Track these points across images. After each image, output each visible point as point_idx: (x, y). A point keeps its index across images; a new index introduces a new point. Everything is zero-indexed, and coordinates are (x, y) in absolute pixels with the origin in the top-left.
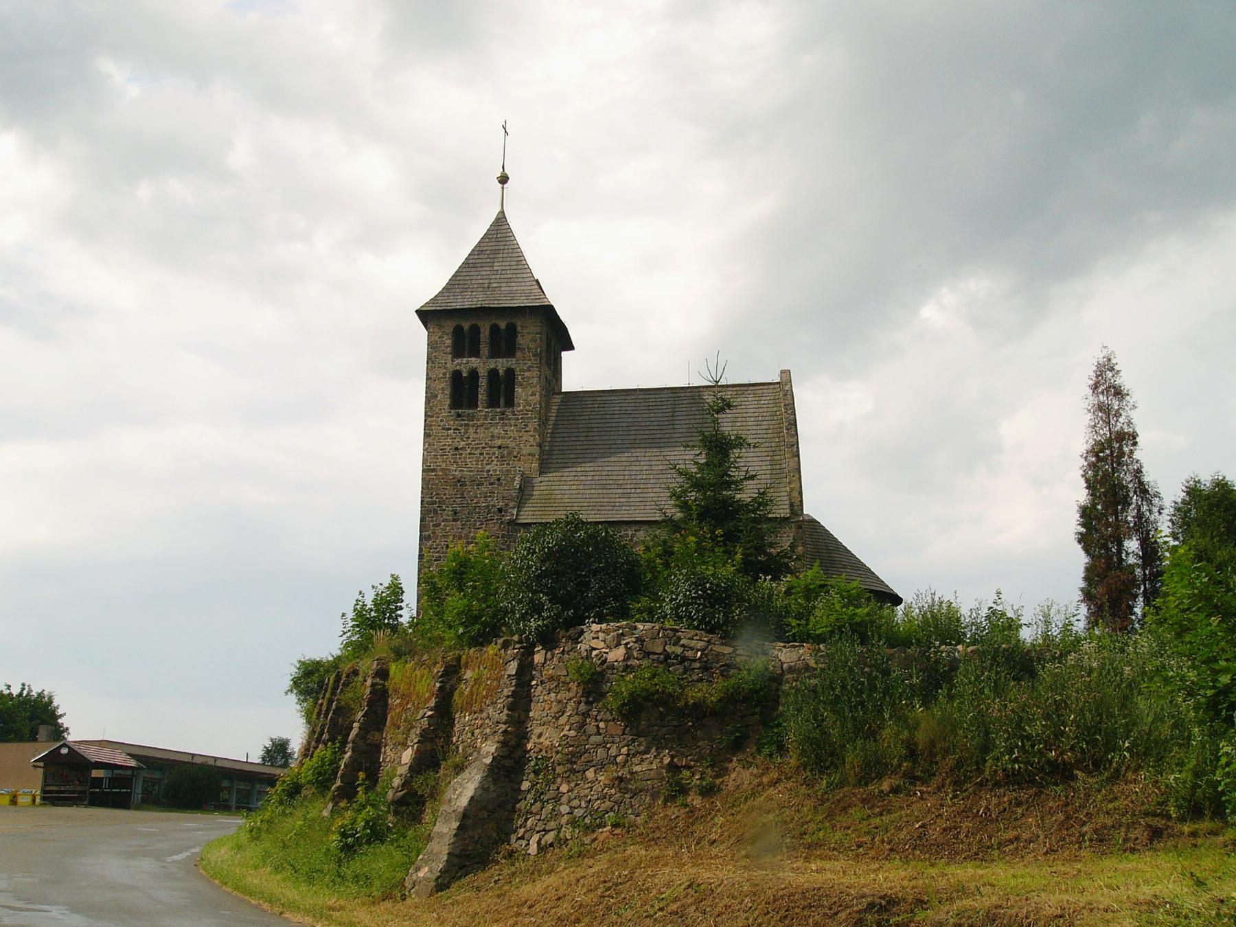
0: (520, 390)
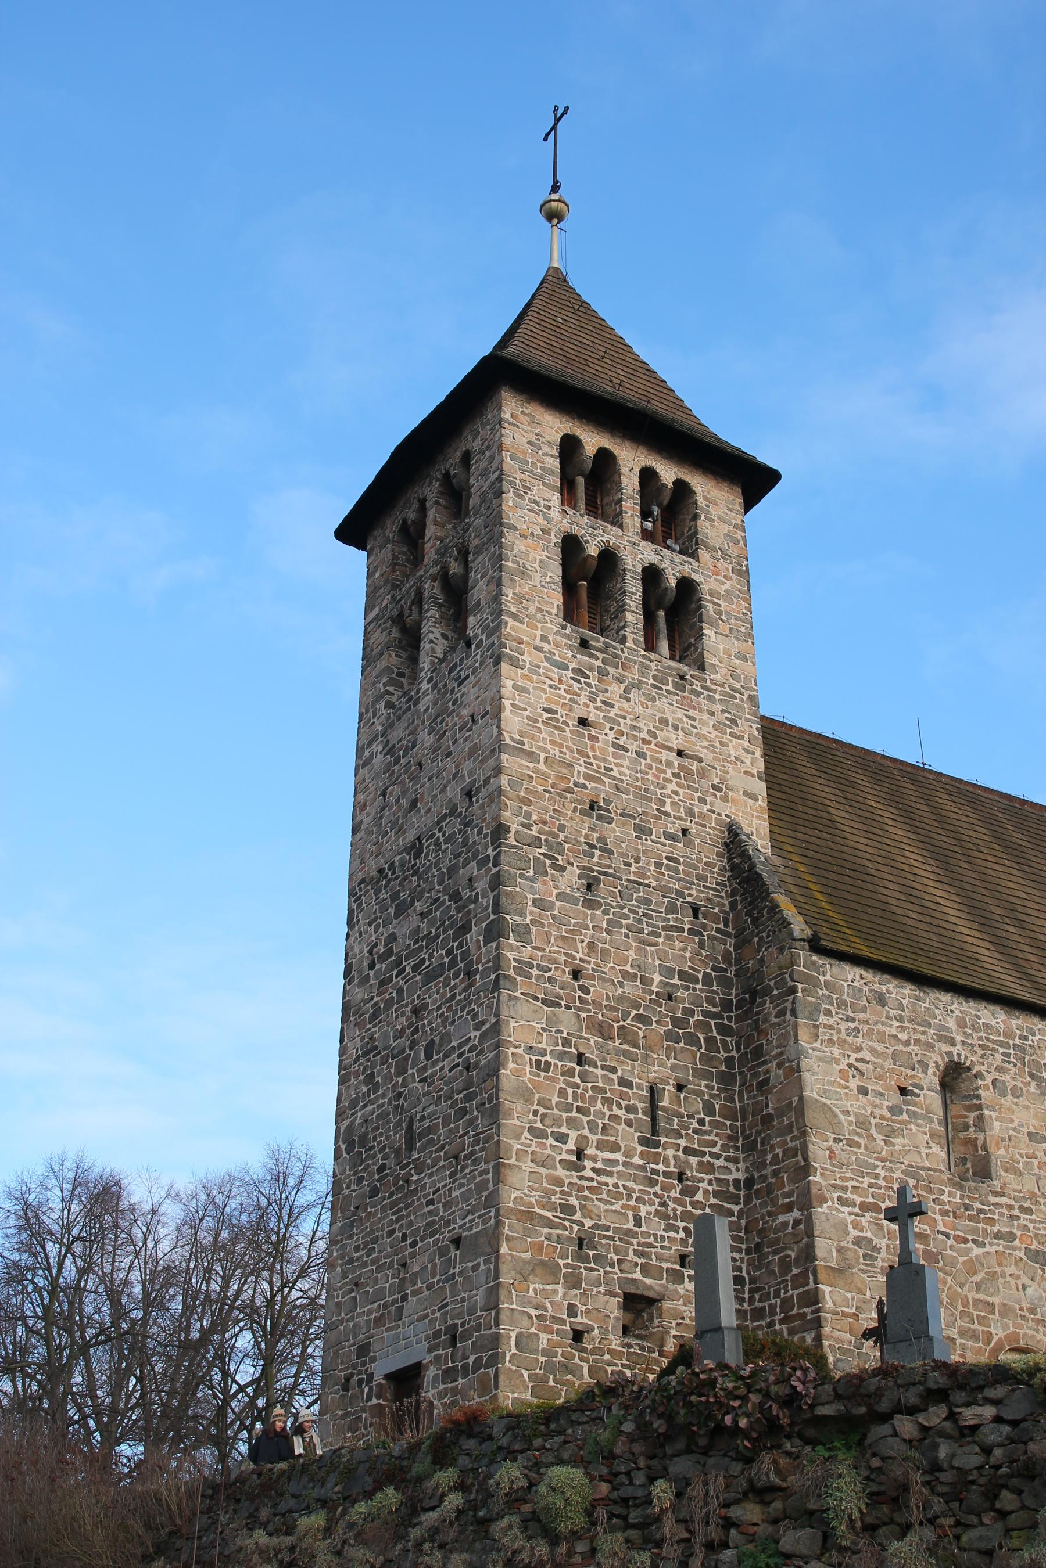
0: (713, 639)
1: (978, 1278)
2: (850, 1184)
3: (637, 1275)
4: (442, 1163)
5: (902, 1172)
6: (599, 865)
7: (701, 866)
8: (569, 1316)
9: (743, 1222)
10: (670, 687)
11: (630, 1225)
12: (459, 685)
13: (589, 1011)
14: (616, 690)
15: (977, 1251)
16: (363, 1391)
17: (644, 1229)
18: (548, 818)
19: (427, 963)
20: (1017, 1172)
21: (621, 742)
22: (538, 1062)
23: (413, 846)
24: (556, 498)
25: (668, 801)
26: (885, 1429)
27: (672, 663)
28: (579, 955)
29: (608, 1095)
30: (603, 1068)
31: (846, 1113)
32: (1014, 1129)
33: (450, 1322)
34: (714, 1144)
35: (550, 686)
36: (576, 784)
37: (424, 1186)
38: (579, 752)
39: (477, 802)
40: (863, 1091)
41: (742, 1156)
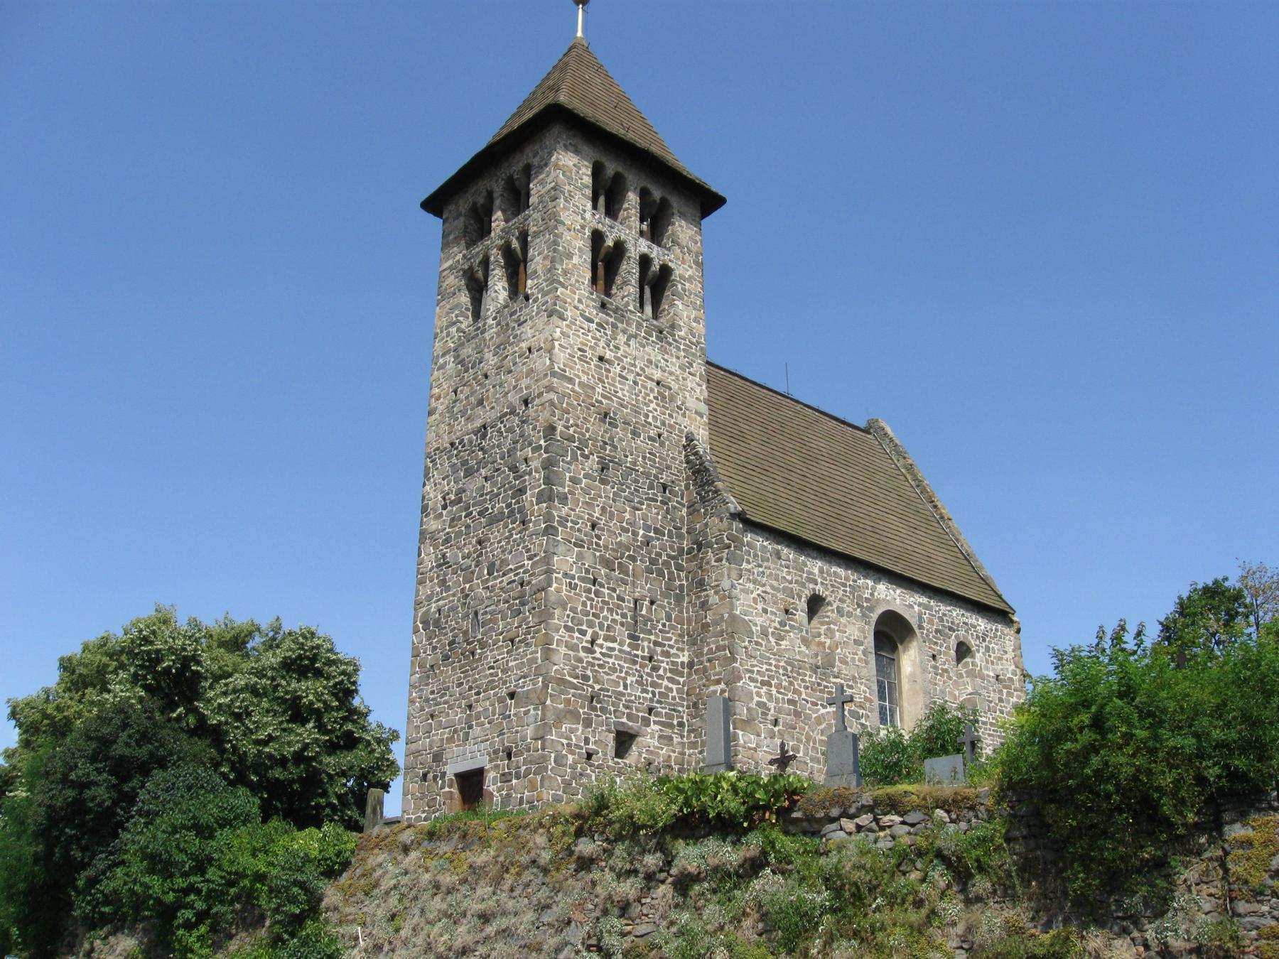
1: (822, 727)
2: (755, 669)
3: (624, 720)
4: (500, 643)
5: (785, 662)
6: (609, 456)
7: (669, 459)
8: (585, 744)
9: (686, 688)
10: (654, 339)
11: (621, 689)
12: (519, 325)
13: (601, 551)
14: (622, 338)
15: (823, 711)
16: (438, 783)
17: (629, 691)
18: (580, 423)
19: (490, 511)
20: (846, 663)
21: (624, 374)
22: (570, 583)
23: (479, 432)
24: (589, 205)
25: (651, 415)
26: (834, 826)
27: (655, 322)
28: (596, 515)
29: (611, 606)
30: (608, 588)
31: (756, 625)
32: (847, 637)
33: (506, 744)
34: (670, 639)
35: (583, 334)
36: (597, 401)
37: (486, 657)
38: (599, 379)
39: (532, 408)
40: (765, 611)
41: (686, 647)
